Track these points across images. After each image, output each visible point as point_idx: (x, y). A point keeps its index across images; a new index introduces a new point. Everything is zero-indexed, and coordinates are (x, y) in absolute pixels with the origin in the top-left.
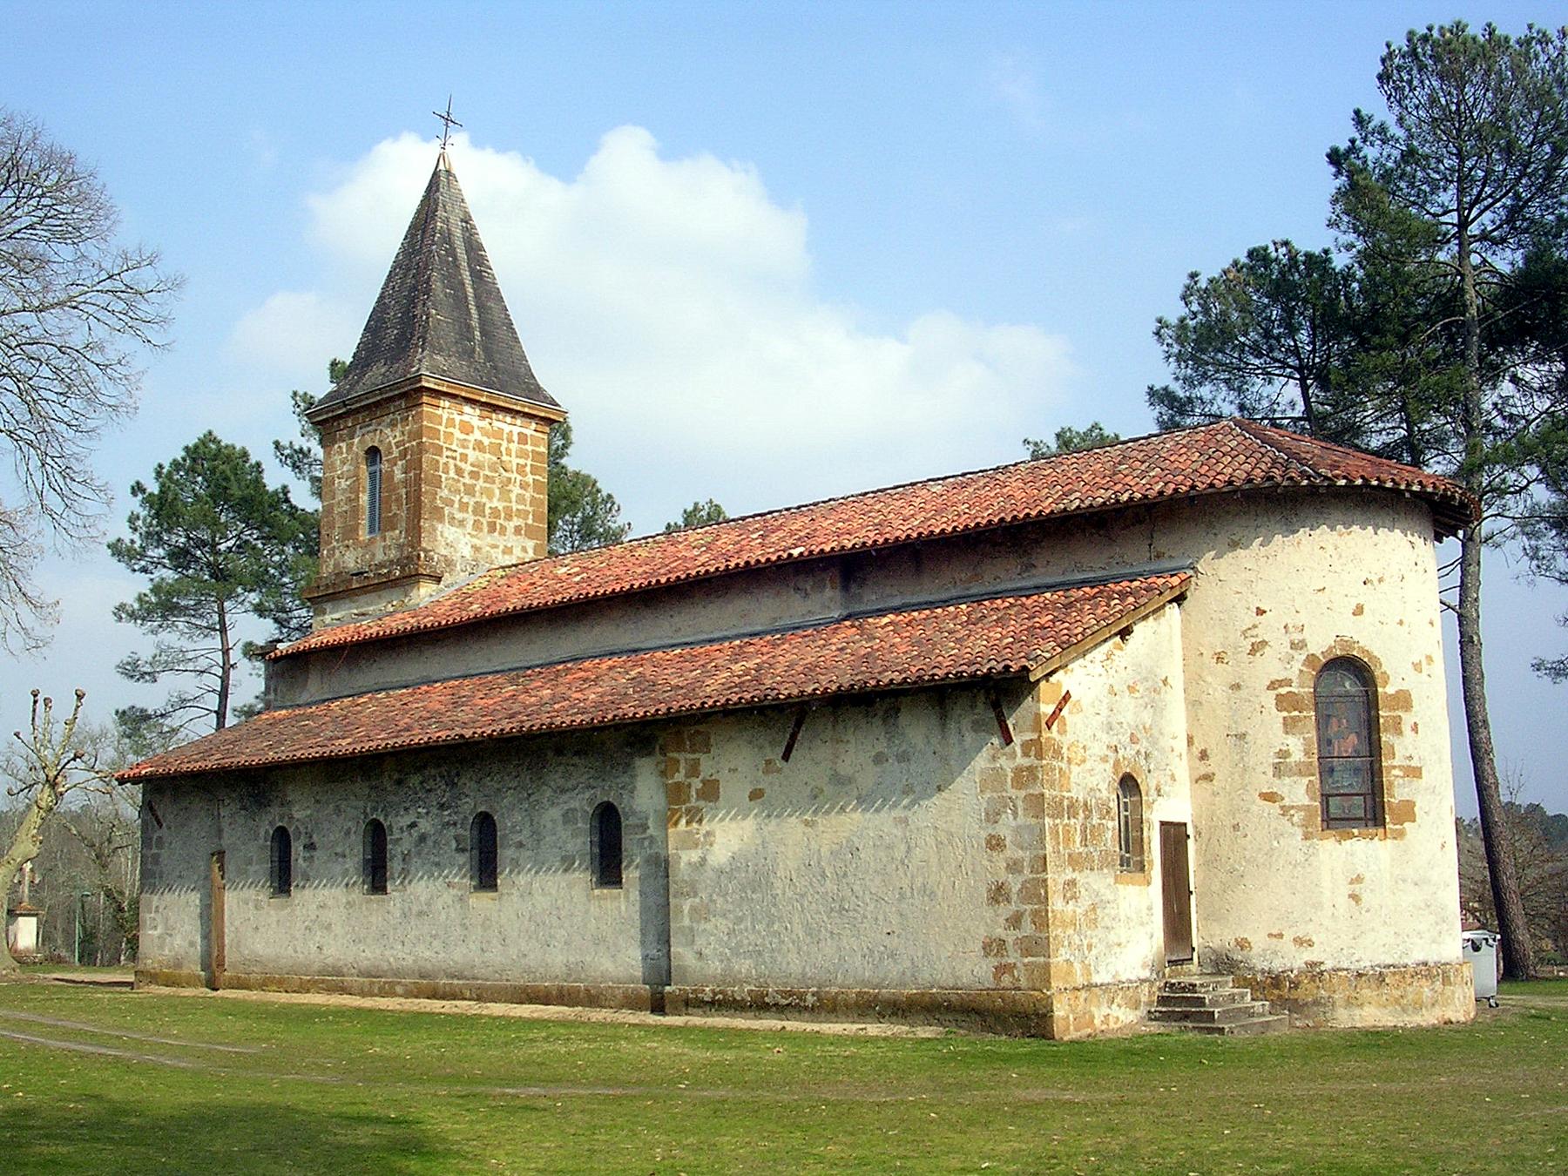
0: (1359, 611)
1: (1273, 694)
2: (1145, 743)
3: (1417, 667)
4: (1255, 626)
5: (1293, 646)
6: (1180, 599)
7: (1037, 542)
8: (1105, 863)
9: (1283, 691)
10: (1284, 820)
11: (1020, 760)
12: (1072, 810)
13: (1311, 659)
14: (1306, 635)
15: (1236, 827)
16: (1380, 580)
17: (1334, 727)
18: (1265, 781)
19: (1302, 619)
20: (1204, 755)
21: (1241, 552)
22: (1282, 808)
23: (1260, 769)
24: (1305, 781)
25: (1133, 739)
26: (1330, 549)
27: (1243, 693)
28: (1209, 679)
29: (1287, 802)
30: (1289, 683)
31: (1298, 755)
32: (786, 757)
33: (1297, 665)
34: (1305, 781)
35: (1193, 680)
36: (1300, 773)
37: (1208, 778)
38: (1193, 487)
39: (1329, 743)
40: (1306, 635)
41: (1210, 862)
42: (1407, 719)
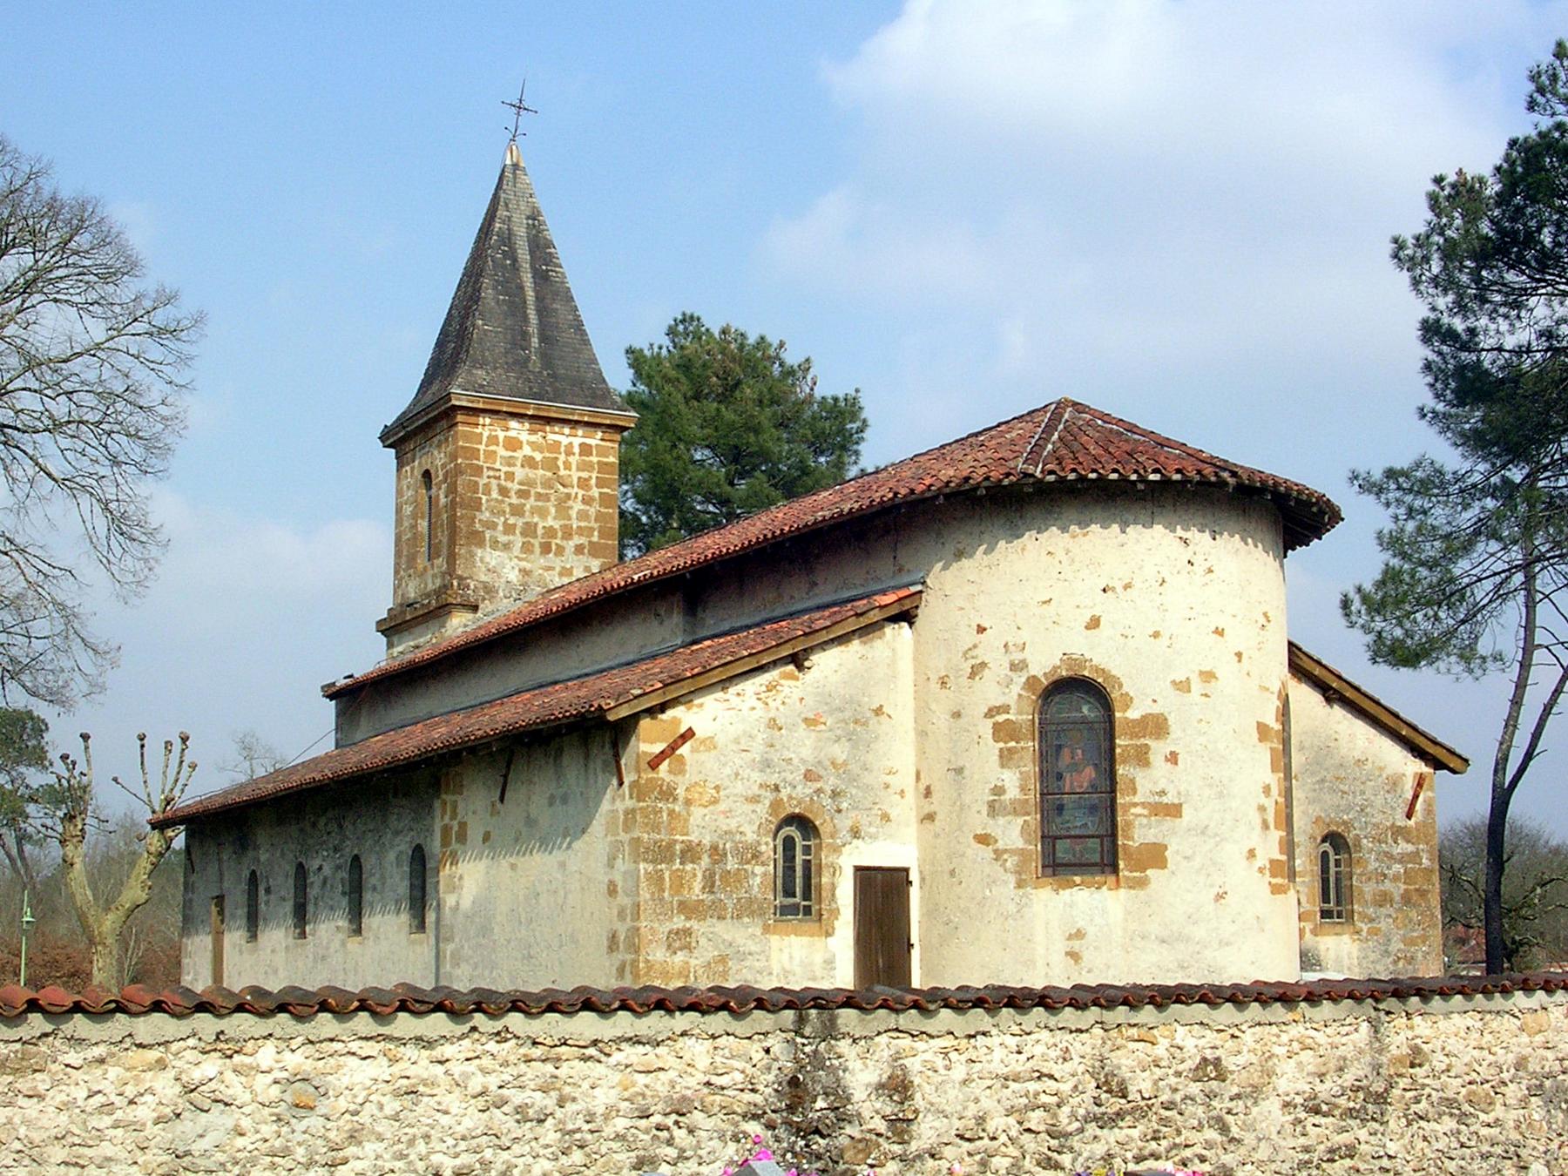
0: (1094, 623)
1: (990, 722)
2: (832, 780)
3: (1183, 686)
4: (975, 646)
5: (1014, 667)
6: (906, 616)
7: (818, 557)
8: (748, 908)
9: (1001, 718)
10: (997, 866)
11: (629, 803)
12: (690, 853)
13: (1031, 682)
14: (1027, 654)
15: (952, 873)
16: (1127, 587)
17: (1066, 758)
18: (979, 821)
19: (1024, 636)
20: (928, 793)
21: (965, 562)
22: (996, 851)
23: (975, 808)
24: (1020, 821)
25: (809, 776)
26: (1060, 554)
27: (962, 721)
28: (934, 707)
29: (1000, 845)
30: (1005, 709)
31: (1013, 793)
32: (502, 799)
33: (1016, 689)
34: (1020, 821)
35: (922, 709)
36: (1015, 813)
37: (930, 817)
38: (912, 491)
39: (1060, 777)
40: (1027, 654)
41: (930, 913)
42: (1158, 749)
